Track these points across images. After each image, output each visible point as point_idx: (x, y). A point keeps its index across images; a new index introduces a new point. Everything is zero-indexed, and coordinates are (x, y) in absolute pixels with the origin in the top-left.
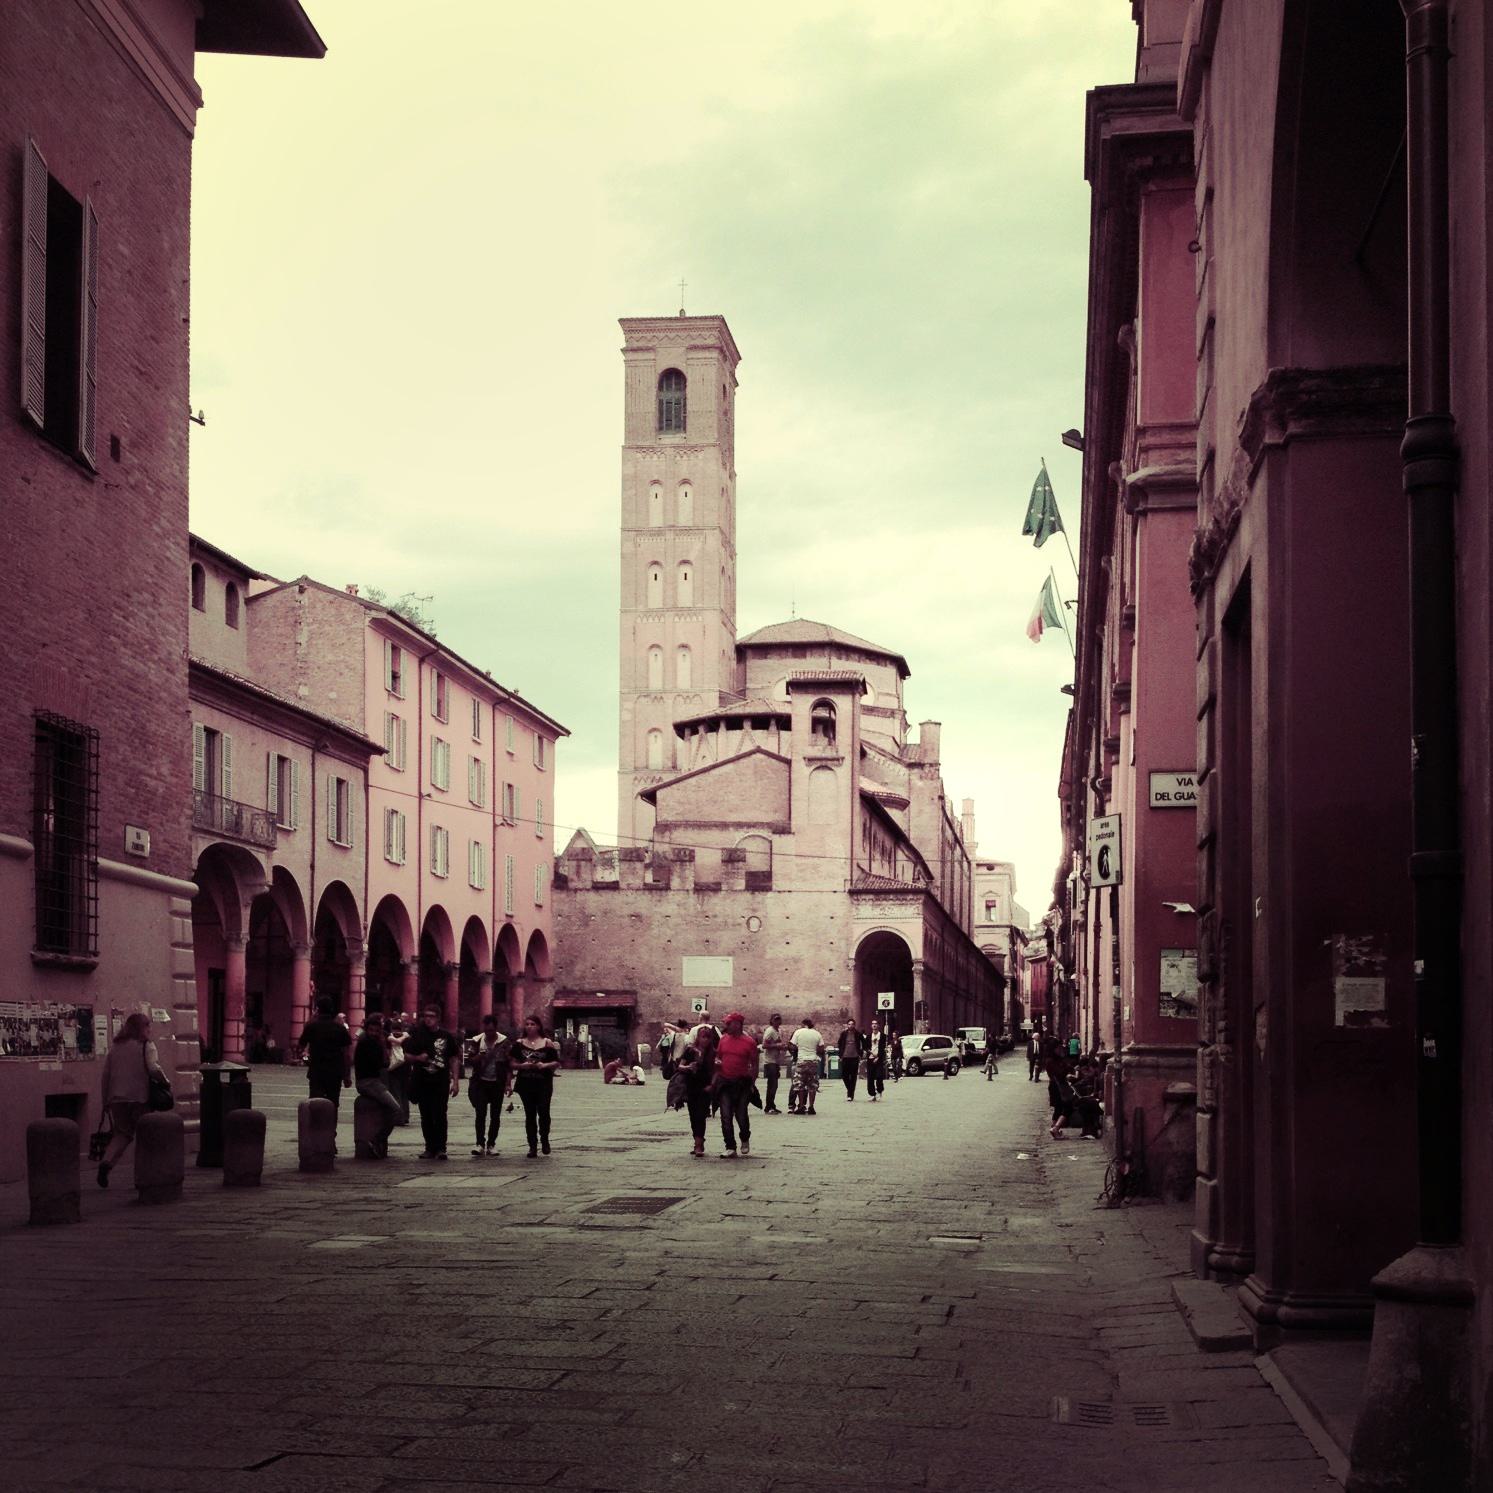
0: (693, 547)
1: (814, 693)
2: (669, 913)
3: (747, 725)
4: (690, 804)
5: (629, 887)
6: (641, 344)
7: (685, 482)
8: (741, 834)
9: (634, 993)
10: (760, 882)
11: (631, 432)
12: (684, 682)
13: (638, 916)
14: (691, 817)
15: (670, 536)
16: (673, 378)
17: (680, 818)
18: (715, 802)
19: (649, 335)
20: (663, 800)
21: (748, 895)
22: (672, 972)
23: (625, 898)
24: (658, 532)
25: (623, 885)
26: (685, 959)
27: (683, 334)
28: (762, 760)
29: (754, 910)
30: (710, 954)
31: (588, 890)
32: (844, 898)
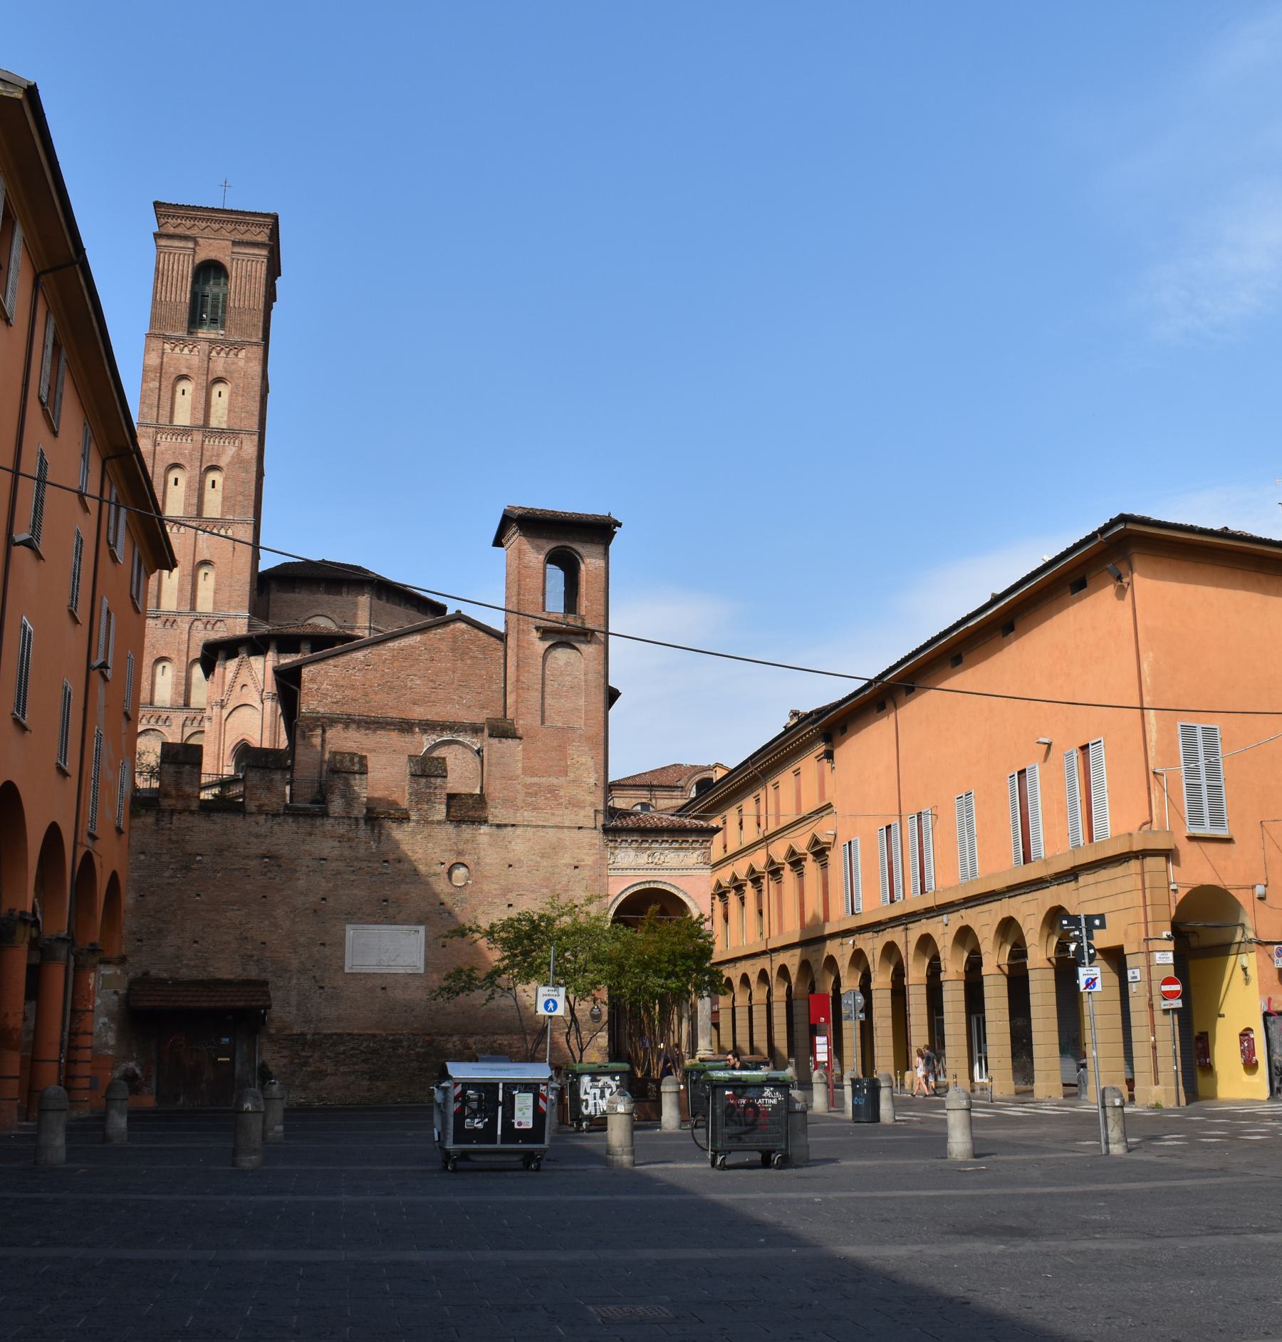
0: (227, 452)
1: (550, 539)
2: (325, 854)
3: (305, 647)
4: (353, 687)
5: (260, 810)
6: (179, 231)
7: (220, 380)
8: (427, 741)
9: (265, 983)
10: (467, 810)
11: (155, 319)
12: (205, 603)
13: (272, 857)
14: (355, 710)
15: (198, 436)
16: (210, 271)
17: (337, 710)
18: (392, 688)
19: (188, 223)
20: (312, 680)
21: (450, 828)
22: (327, 951)
23: (255, 829)
24: (186, 431)
25: (252, 806)
26: (348, 927)
27: (230, 227)
28: (463, 632)
29: (460, 853)
30: (392, 920)
31: (192, 813)
32: (597, 837)
